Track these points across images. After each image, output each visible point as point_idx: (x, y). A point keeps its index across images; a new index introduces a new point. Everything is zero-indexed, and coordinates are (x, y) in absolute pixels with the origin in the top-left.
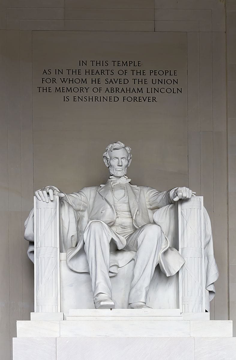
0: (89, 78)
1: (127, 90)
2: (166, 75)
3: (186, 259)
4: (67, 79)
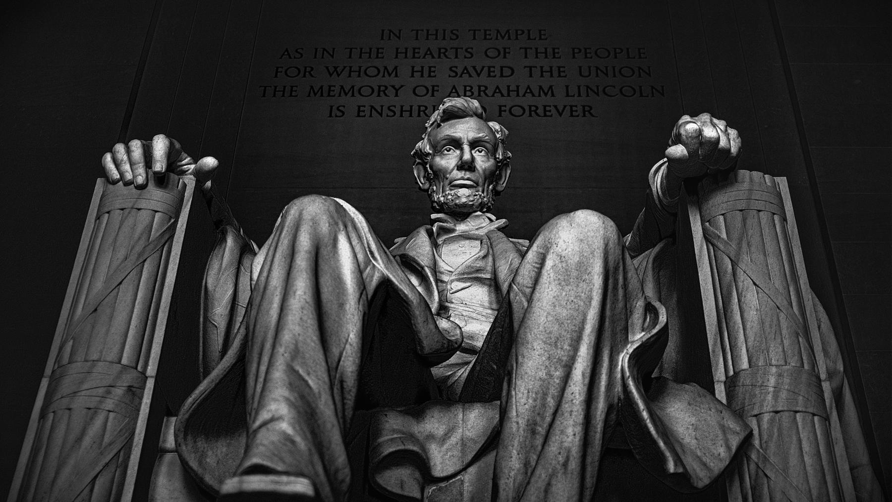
1: (509, 91)
3: (754, 424)
4: (345, 67)
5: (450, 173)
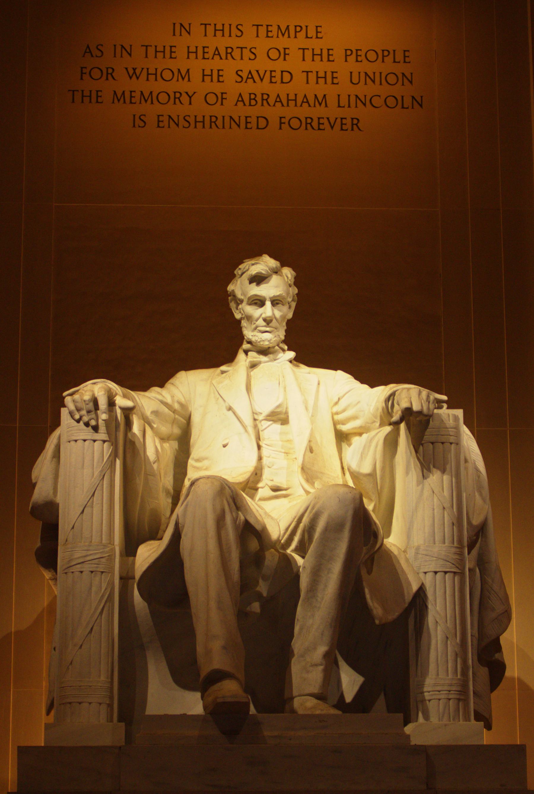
0: (196, 66)
1: (288, 100)
2: (383, 61)
4: (143, 69)
5: (257, 320)
